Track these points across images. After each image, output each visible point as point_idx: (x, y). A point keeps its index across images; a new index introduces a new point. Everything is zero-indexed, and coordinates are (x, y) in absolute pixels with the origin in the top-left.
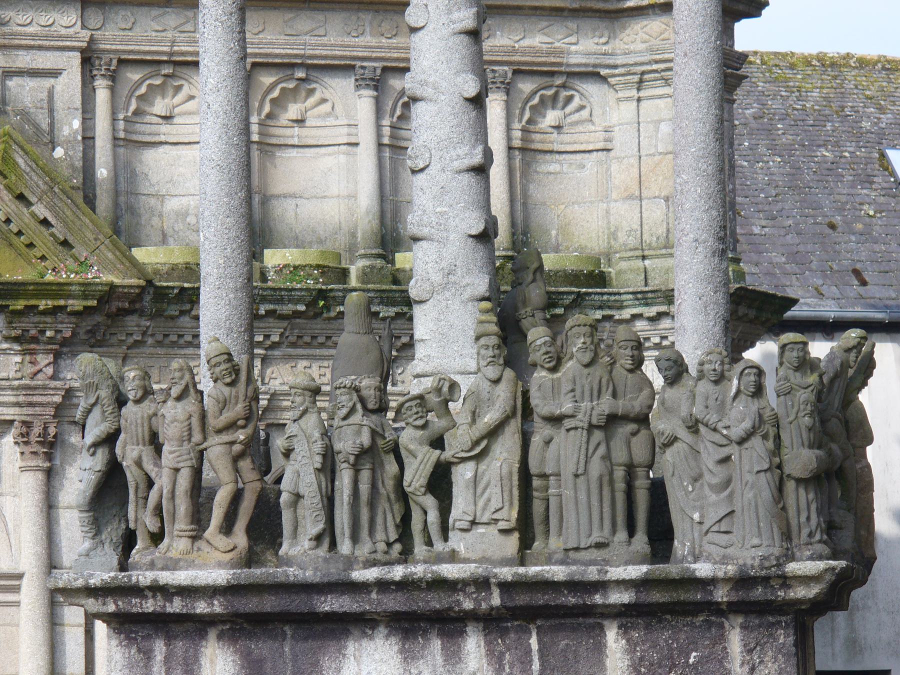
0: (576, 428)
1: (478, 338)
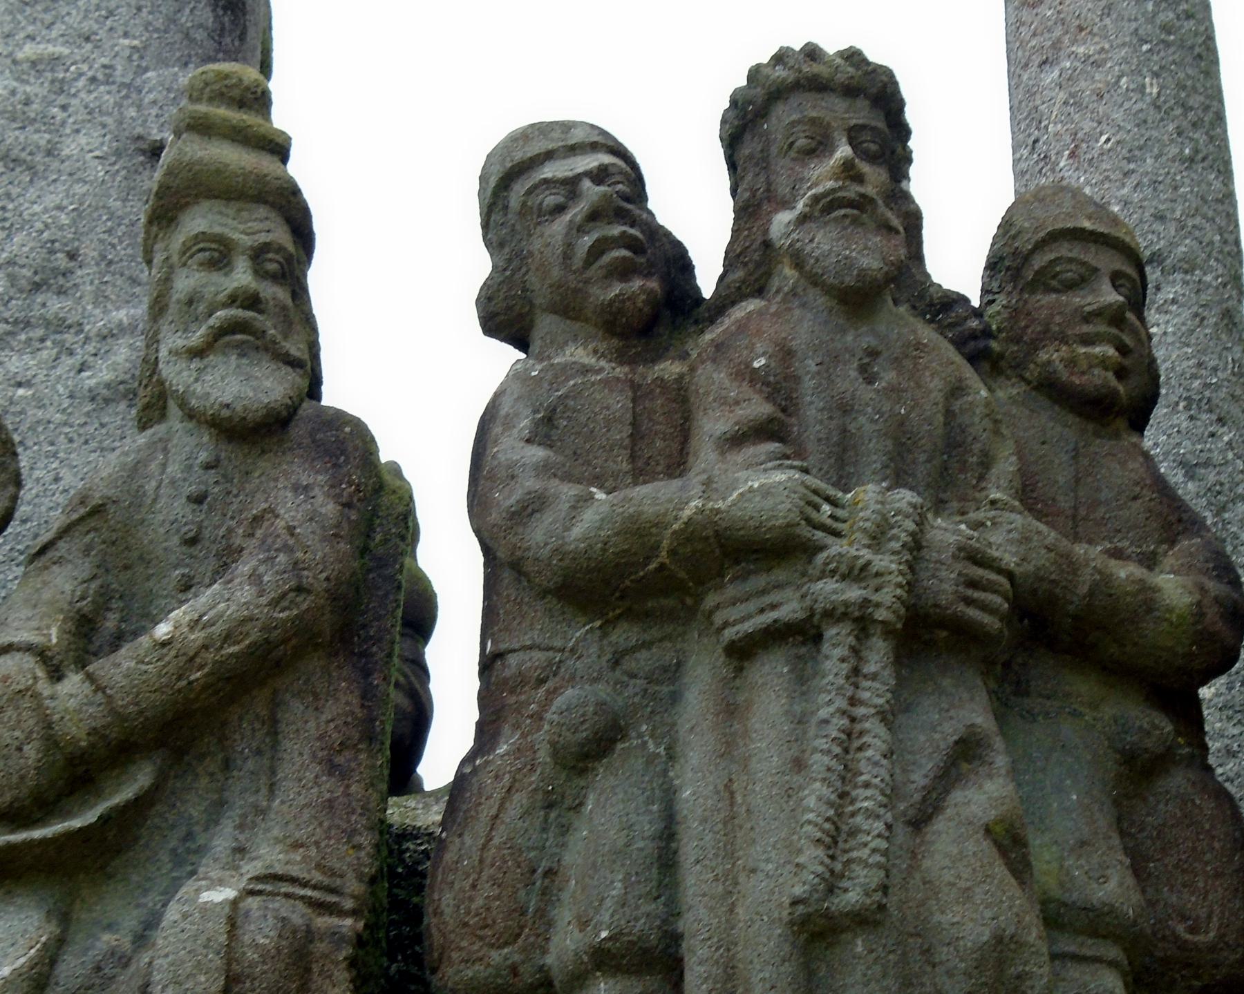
0: (803, 634)
1: (166, 211)
